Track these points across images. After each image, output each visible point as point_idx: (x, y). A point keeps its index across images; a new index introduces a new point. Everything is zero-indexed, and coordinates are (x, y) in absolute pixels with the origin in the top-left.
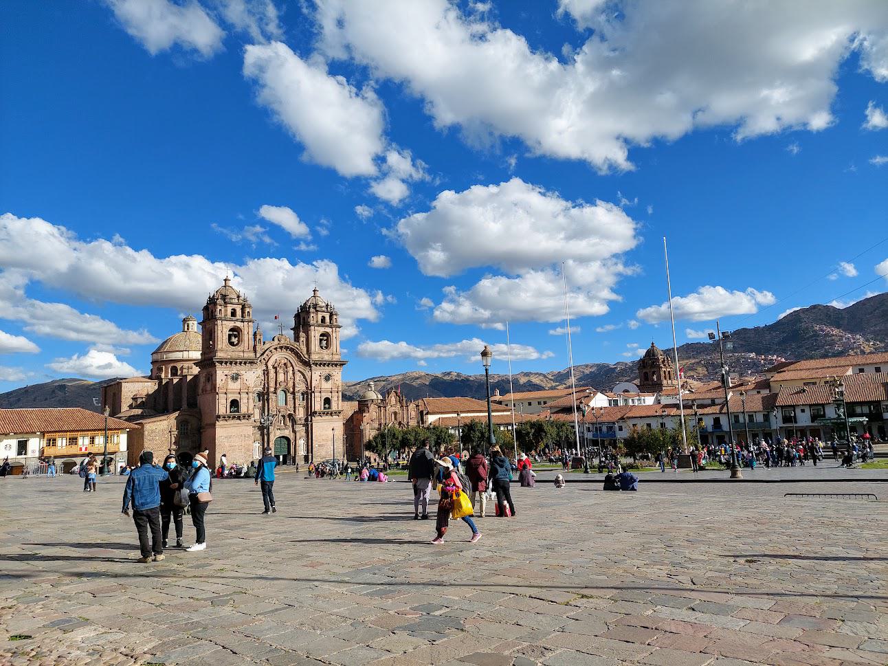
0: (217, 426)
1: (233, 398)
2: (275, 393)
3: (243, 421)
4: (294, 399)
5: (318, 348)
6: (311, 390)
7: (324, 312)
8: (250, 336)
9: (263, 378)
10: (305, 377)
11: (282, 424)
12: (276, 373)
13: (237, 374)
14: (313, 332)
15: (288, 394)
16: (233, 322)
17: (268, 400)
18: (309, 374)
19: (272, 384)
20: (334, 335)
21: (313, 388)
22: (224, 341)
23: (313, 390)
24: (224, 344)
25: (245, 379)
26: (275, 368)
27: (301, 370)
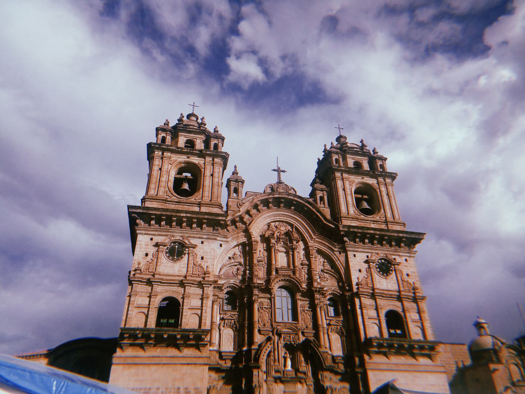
0: (114, 361)
3: (187, 352)
4: (313, 307)
5: (352, 210)
11: (289, 367)
12: (269, 250)
14: (339, 183)
15: (298, 296)
16: (185, 157)
17: (251, 304)
19: (261, 273)
20: (383, 189)
22: (163, 184)
23: (355, 290)
24: (162, 189)
25: (199, 257)
26: (266, 240)
27: (323, 248)
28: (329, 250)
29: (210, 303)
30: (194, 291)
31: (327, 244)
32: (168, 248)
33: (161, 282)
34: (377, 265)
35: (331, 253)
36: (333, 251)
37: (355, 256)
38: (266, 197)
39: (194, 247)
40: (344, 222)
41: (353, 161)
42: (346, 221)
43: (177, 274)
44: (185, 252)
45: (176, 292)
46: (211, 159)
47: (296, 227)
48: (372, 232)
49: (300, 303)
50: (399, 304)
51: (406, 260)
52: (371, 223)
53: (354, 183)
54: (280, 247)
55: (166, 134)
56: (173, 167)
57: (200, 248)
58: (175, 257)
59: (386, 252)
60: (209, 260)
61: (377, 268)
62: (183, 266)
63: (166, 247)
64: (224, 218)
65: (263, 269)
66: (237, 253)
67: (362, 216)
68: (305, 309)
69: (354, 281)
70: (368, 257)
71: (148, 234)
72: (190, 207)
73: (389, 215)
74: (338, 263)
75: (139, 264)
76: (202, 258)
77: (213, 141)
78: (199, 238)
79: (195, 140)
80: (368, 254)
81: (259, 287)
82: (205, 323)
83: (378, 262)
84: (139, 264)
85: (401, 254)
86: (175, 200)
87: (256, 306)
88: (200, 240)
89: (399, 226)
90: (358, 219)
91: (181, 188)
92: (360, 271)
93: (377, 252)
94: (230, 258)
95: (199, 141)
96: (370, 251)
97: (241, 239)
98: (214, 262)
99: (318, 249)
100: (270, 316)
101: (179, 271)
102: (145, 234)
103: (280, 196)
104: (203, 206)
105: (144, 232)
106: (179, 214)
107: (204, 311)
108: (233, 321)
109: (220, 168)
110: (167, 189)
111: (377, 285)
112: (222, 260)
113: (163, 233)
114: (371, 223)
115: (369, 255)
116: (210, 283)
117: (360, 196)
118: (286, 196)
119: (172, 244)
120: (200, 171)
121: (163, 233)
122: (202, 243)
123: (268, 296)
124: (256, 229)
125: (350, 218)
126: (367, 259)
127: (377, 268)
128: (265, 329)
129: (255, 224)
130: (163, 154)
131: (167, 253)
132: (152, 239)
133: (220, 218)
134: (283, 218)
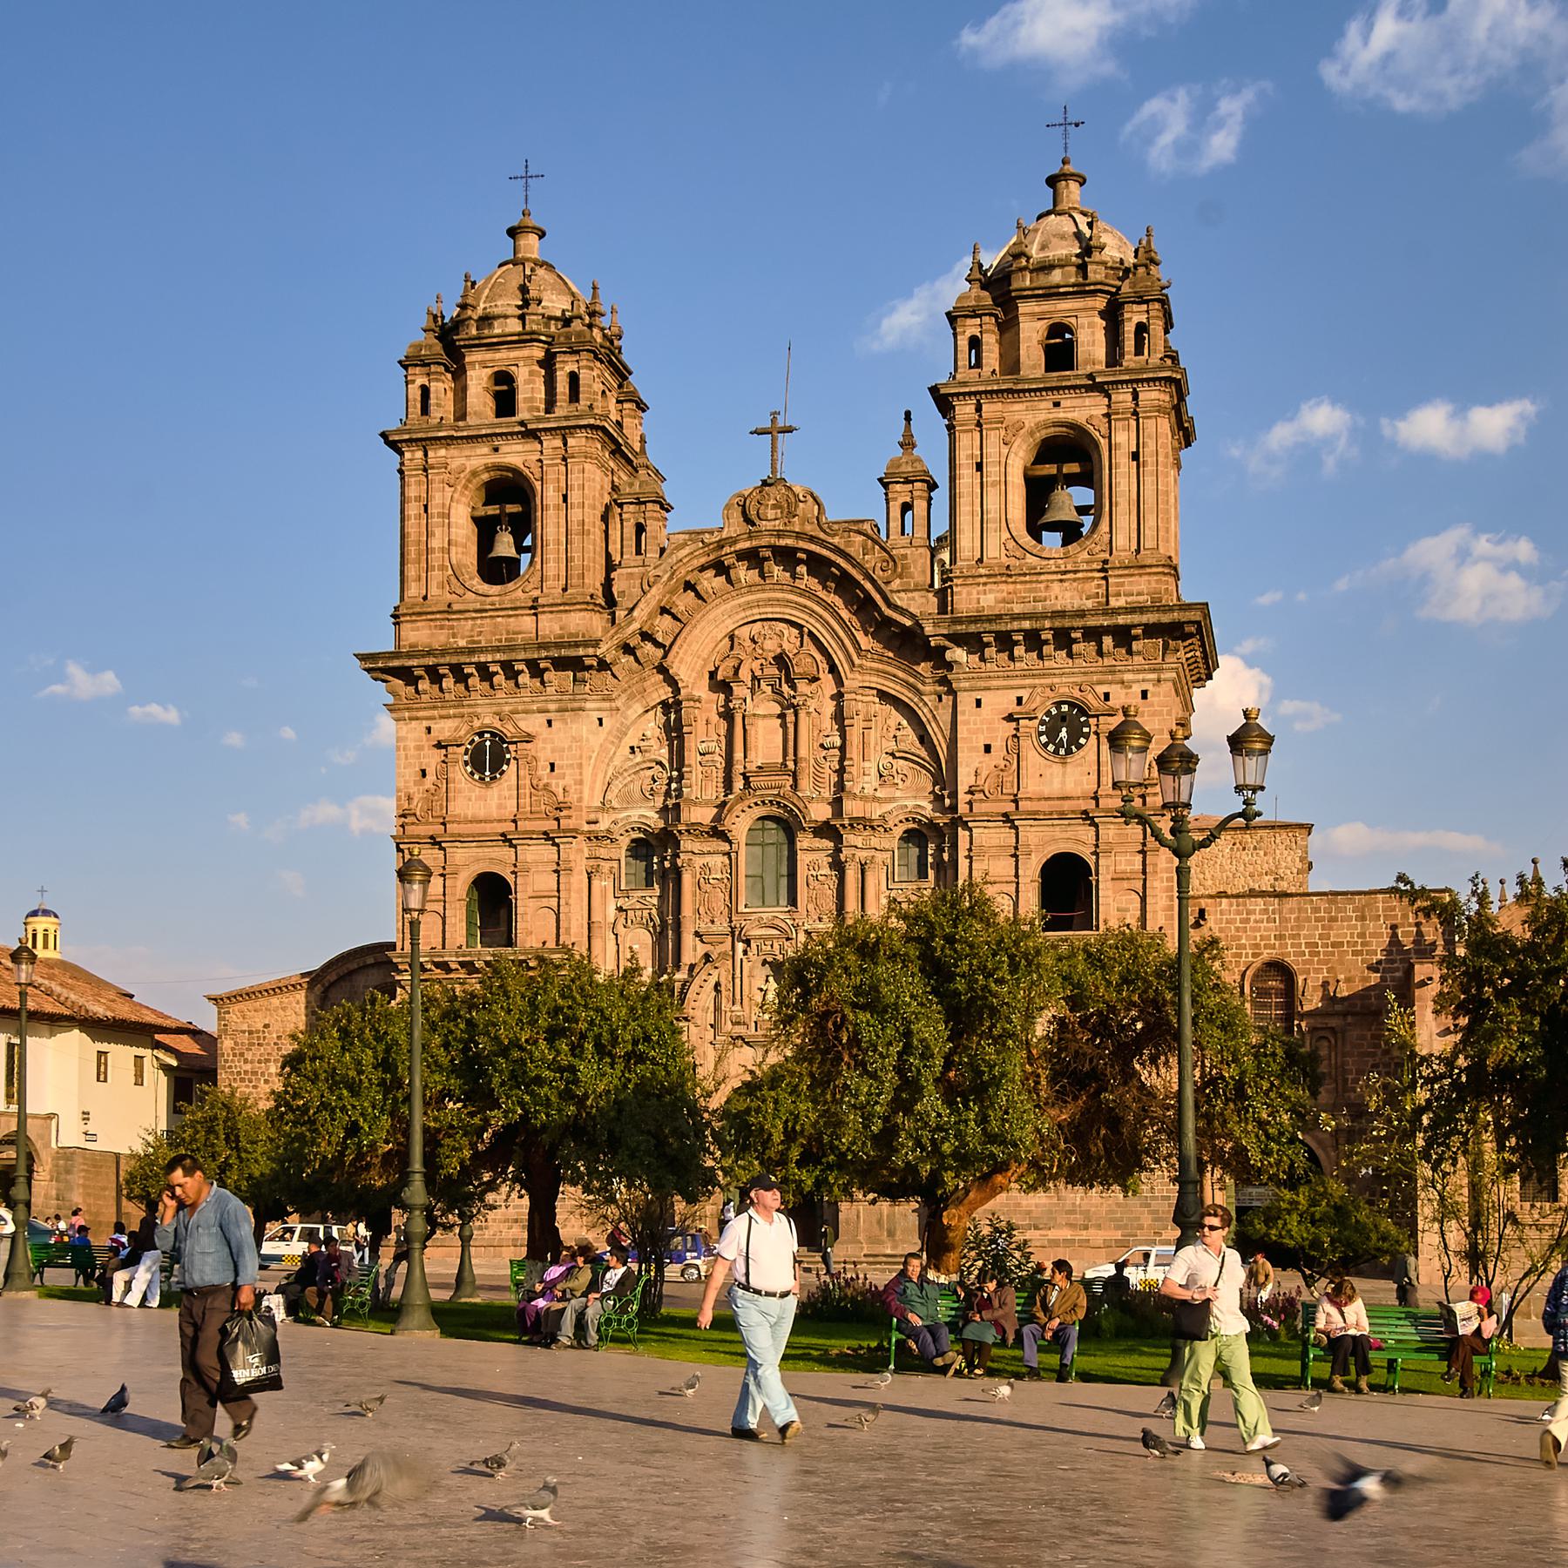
1: (485, 868)
2: (717, 833)
6: (954, 808)
7: (1052, 293)
8: (576, 515)
9: (663, 754)
10: (924, 739)
13: (498, 739)
16: (485, 450)
17: (677, 872)
18: (944, 716)
19: (703, 789)
21: (963, 798)
23: (963, 808)
24: (436, 575)
26: (721, 686)
28: (910, 690)
29: (578, 880)
30: (537, 854)
31: (900, 674)
32: (467, 749)
33: (459, 840)
34: (1042, 723)
35: (916, 700)
36: (919, 693)
37: (978, 703)
38: (712, 557)
39: (529, 739)
40: (960, 593)
41: (1042, 326)
42: (969, 588)
43: (495, 815)
44: (508, 756)
45: (497, 860)
46: (558, 443)
47: (811, 634)
48: (1026, 625)
49: (803, 859)
50: (1088, 833)
51: (1144, 694)
52: (1052, 581)
53: (1022, 432)
54: (761, 708)
55: (428, 375)
56: (456, 496)
57: (545, 741)
58: (487, 773)
59: (1078, 679)
60: (568, 772)
61: (1041, 734)
62: (506, 793)
63: (463, 748)
64: (591, 651)
65: (714, 775)
66: (648, 734)
67: (1030, 559)
68: (820, 872)
69: (965, 780)
70: (1019, 701)
71: (417, 719)
72: (512, 620)
73: (1121, 540)
74: (932, 729)
75: (409, 799)
76: (552, 766)
77: (562, 369)
78: (540, 711)
79: (513, 368)
80: (1020, 693)
81: (694, 830)
82: (568, 930)
83: (1048, 713)
84: (409, 799)
85: (1128, 677)
86: (471, 607)
87: (687, 879)
88: (542, 718)
89: (1146, 578)
90: (1007, 573)
91: (493, 555)
92: (988, 749)
93: (1048, 681)
94: (632, 748)
95: (527, 369)
96: (1028, 682)
97: (655, 695)
98: (581, 774)
99: (878, 690)
100: (727, 898)
101: (500, 806)
102: (411, 719)
103: (755, 543)
104: (544, 612)
105: (407, 714)
106: (475, 659)
107: (562, 902)
108: (646, 913)
109: (587, 466)
110: (450, 572)
111: (1030, 786)
112: (607, 761)
113: (451, 712)
114: (1052, 581)
115: (1025, 694)
116: (574, 833)
117: (1050, 469)
118: (773, 541)
119: (477, 739)
120: (533, 489)
121: (451, 712)
122: (549, 723)
123: (726, 847)
124: (689, 659)
125: (981, 576)
126: (1019, 709)
127: (1041, 734)
128: (716, 929)
129: (685, 646)
130: (426, 455)
131: (466, 763)
132: (429, 730)
133: (581, 652)
134: (770, 610)
